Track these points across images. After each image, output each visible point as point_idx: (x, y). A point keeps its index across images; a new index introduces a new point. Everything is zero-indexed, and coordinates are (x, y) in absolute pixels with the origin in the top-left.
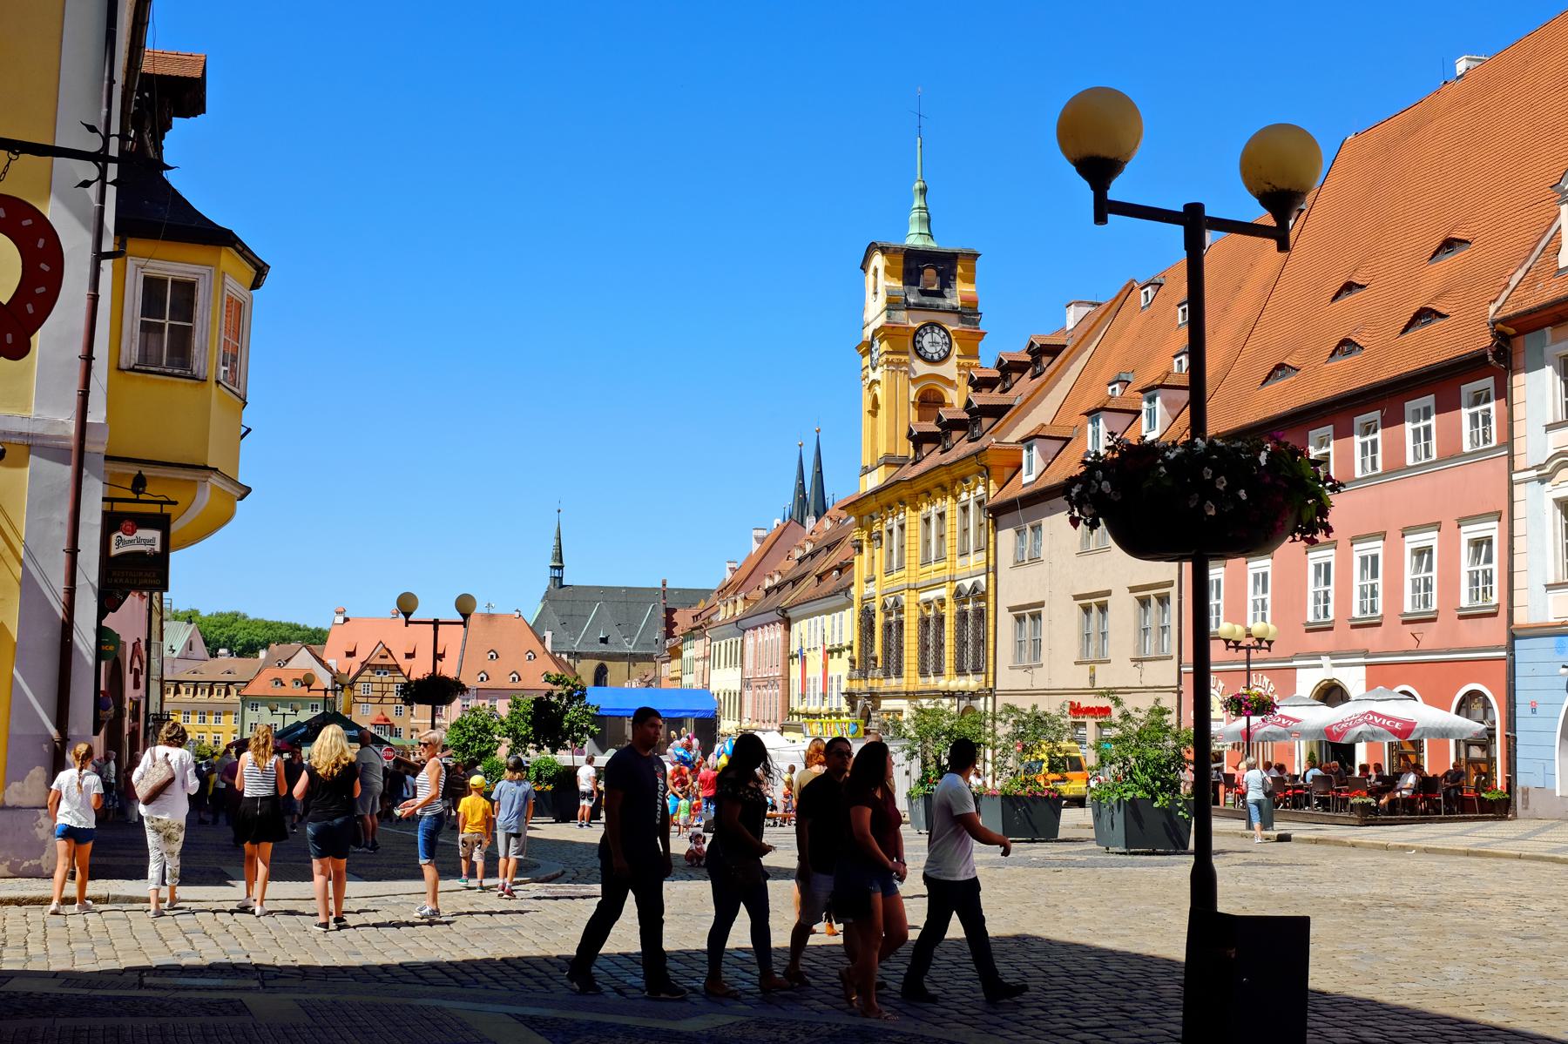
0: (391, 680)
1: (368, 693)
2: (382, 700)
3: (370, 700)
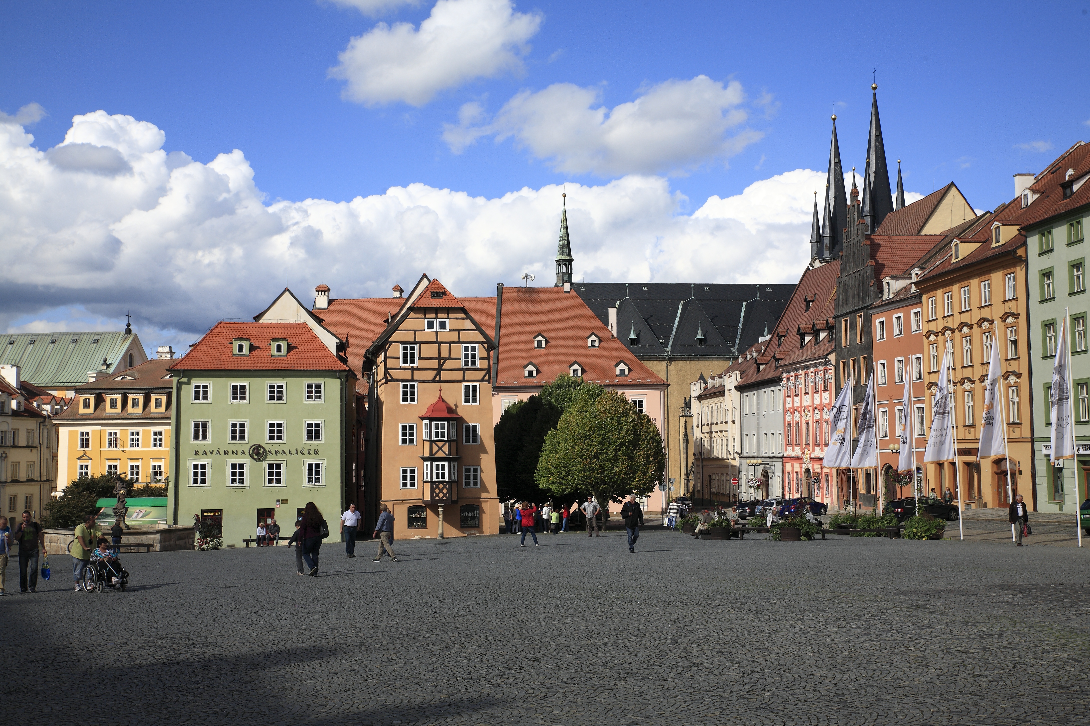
0: (454, 337)
1: (413, 362)
2: (439, 374)
3: (417, 375)
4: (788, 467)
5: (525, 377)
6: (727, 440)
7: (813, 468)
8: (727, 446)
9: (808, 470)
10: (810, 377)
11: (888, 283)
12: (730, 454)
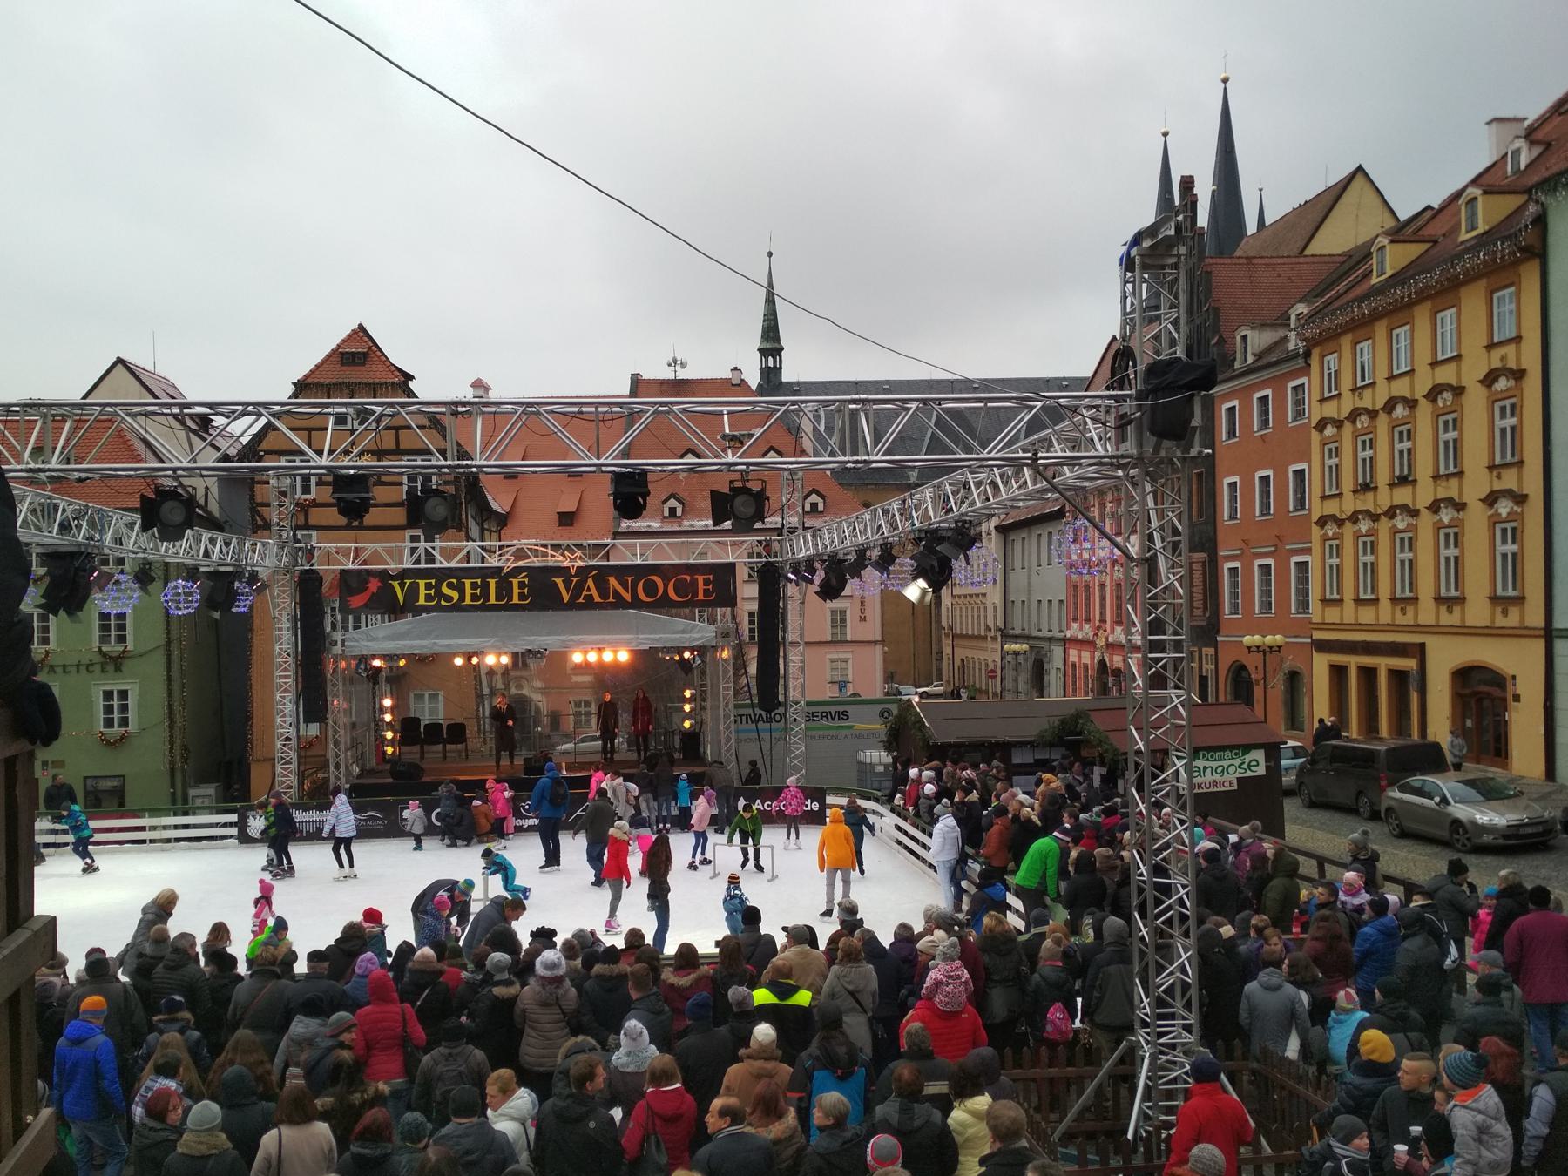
4: (1073, 655)
5: (665, 517)
6: (985, 608)
7: (1111, 661)
8: (986, 617)
9: (1102, 663)
10: (1108, 509)
11: (1245, 338)
12: (990, 630)
